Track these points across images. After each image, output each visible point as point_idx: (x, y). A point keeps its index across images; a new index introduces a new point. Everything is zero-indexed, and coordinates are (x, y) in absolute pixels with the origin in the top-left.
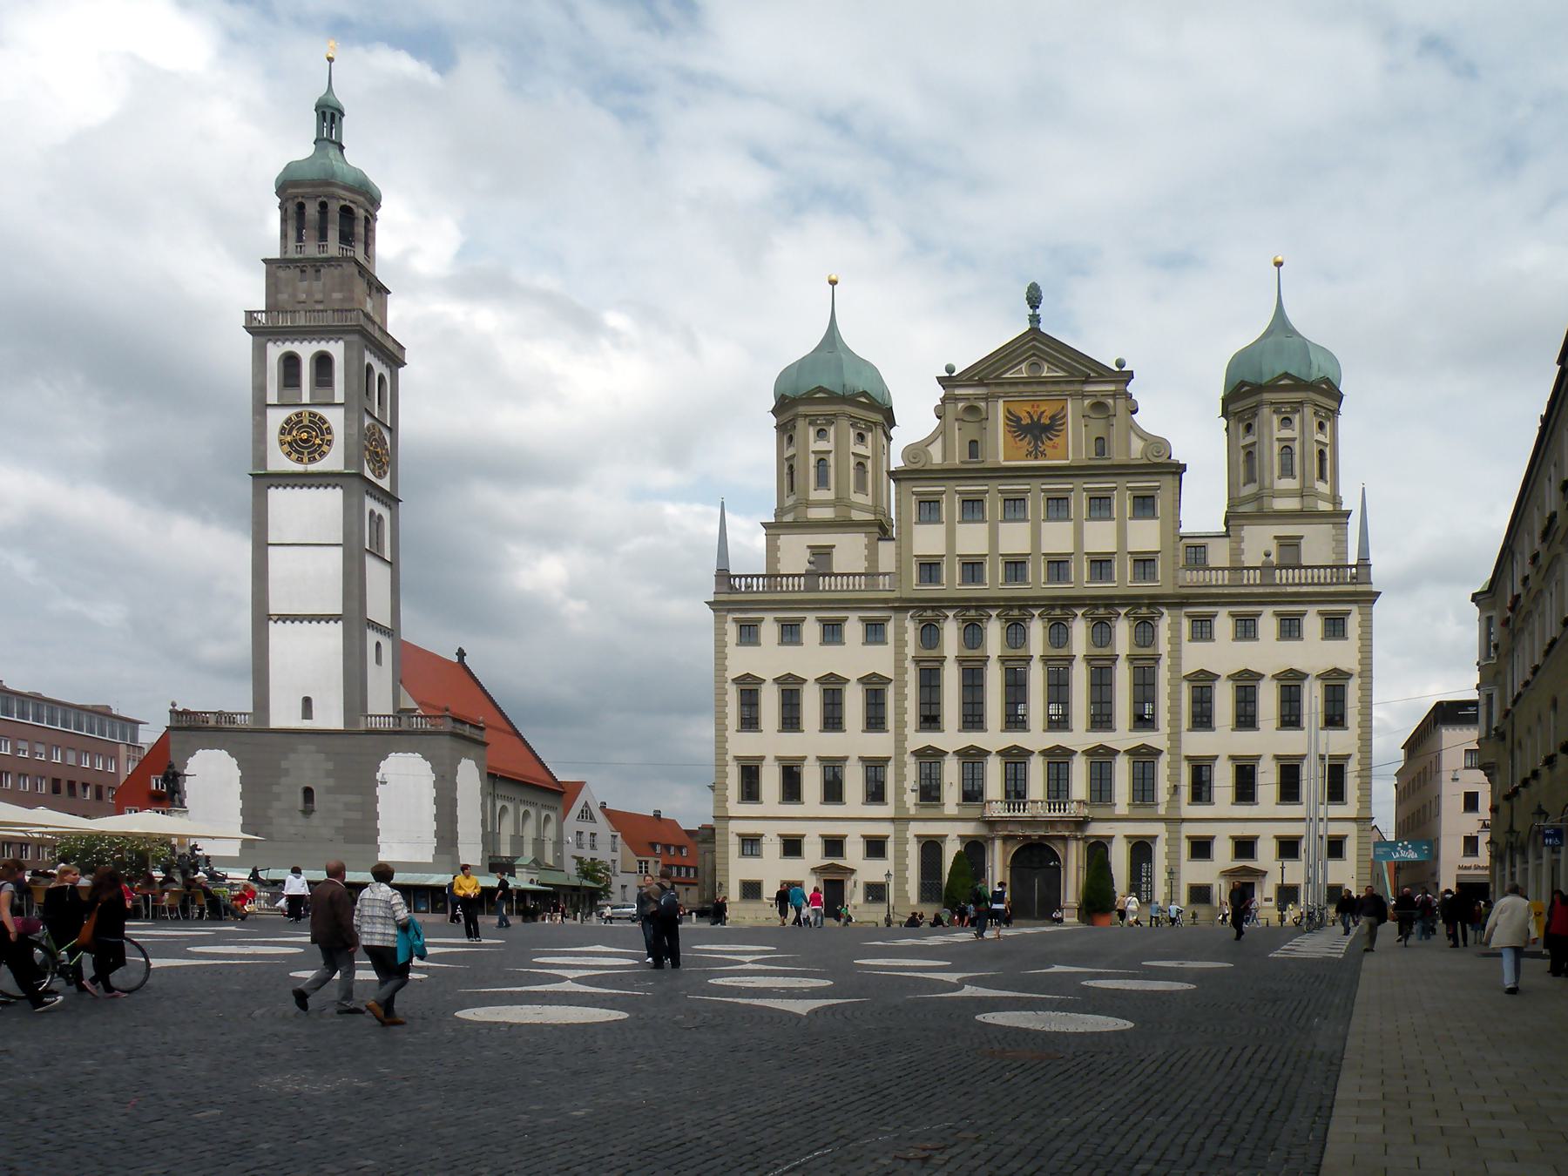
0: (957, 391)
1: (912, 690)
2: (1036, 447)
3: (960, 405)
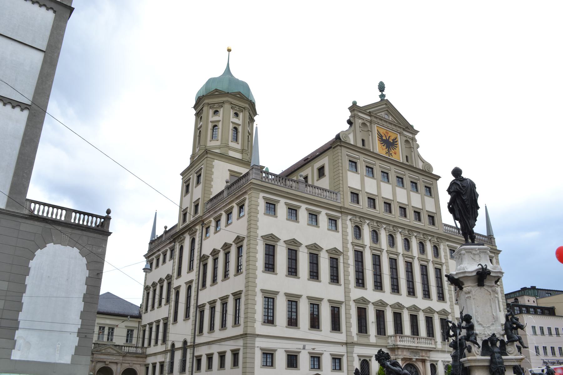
0: (360, 114)
1: (351, 261)
2: (389, 151)
3: (360, 121)
